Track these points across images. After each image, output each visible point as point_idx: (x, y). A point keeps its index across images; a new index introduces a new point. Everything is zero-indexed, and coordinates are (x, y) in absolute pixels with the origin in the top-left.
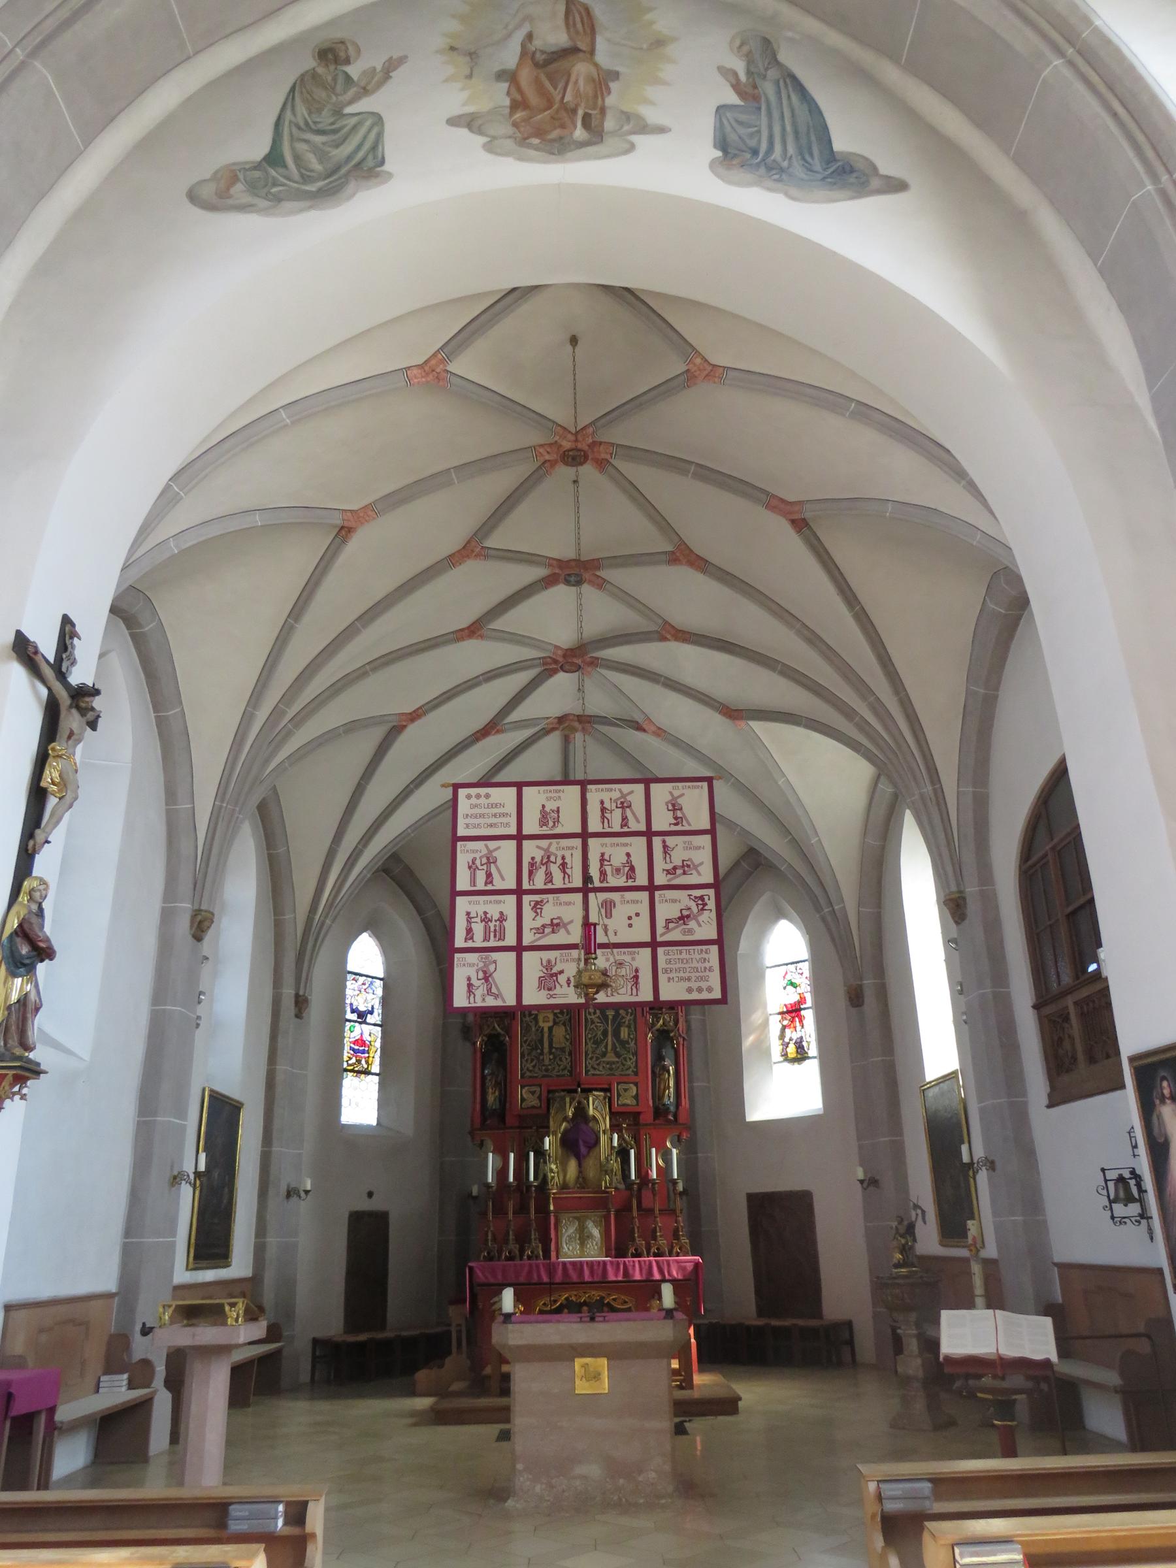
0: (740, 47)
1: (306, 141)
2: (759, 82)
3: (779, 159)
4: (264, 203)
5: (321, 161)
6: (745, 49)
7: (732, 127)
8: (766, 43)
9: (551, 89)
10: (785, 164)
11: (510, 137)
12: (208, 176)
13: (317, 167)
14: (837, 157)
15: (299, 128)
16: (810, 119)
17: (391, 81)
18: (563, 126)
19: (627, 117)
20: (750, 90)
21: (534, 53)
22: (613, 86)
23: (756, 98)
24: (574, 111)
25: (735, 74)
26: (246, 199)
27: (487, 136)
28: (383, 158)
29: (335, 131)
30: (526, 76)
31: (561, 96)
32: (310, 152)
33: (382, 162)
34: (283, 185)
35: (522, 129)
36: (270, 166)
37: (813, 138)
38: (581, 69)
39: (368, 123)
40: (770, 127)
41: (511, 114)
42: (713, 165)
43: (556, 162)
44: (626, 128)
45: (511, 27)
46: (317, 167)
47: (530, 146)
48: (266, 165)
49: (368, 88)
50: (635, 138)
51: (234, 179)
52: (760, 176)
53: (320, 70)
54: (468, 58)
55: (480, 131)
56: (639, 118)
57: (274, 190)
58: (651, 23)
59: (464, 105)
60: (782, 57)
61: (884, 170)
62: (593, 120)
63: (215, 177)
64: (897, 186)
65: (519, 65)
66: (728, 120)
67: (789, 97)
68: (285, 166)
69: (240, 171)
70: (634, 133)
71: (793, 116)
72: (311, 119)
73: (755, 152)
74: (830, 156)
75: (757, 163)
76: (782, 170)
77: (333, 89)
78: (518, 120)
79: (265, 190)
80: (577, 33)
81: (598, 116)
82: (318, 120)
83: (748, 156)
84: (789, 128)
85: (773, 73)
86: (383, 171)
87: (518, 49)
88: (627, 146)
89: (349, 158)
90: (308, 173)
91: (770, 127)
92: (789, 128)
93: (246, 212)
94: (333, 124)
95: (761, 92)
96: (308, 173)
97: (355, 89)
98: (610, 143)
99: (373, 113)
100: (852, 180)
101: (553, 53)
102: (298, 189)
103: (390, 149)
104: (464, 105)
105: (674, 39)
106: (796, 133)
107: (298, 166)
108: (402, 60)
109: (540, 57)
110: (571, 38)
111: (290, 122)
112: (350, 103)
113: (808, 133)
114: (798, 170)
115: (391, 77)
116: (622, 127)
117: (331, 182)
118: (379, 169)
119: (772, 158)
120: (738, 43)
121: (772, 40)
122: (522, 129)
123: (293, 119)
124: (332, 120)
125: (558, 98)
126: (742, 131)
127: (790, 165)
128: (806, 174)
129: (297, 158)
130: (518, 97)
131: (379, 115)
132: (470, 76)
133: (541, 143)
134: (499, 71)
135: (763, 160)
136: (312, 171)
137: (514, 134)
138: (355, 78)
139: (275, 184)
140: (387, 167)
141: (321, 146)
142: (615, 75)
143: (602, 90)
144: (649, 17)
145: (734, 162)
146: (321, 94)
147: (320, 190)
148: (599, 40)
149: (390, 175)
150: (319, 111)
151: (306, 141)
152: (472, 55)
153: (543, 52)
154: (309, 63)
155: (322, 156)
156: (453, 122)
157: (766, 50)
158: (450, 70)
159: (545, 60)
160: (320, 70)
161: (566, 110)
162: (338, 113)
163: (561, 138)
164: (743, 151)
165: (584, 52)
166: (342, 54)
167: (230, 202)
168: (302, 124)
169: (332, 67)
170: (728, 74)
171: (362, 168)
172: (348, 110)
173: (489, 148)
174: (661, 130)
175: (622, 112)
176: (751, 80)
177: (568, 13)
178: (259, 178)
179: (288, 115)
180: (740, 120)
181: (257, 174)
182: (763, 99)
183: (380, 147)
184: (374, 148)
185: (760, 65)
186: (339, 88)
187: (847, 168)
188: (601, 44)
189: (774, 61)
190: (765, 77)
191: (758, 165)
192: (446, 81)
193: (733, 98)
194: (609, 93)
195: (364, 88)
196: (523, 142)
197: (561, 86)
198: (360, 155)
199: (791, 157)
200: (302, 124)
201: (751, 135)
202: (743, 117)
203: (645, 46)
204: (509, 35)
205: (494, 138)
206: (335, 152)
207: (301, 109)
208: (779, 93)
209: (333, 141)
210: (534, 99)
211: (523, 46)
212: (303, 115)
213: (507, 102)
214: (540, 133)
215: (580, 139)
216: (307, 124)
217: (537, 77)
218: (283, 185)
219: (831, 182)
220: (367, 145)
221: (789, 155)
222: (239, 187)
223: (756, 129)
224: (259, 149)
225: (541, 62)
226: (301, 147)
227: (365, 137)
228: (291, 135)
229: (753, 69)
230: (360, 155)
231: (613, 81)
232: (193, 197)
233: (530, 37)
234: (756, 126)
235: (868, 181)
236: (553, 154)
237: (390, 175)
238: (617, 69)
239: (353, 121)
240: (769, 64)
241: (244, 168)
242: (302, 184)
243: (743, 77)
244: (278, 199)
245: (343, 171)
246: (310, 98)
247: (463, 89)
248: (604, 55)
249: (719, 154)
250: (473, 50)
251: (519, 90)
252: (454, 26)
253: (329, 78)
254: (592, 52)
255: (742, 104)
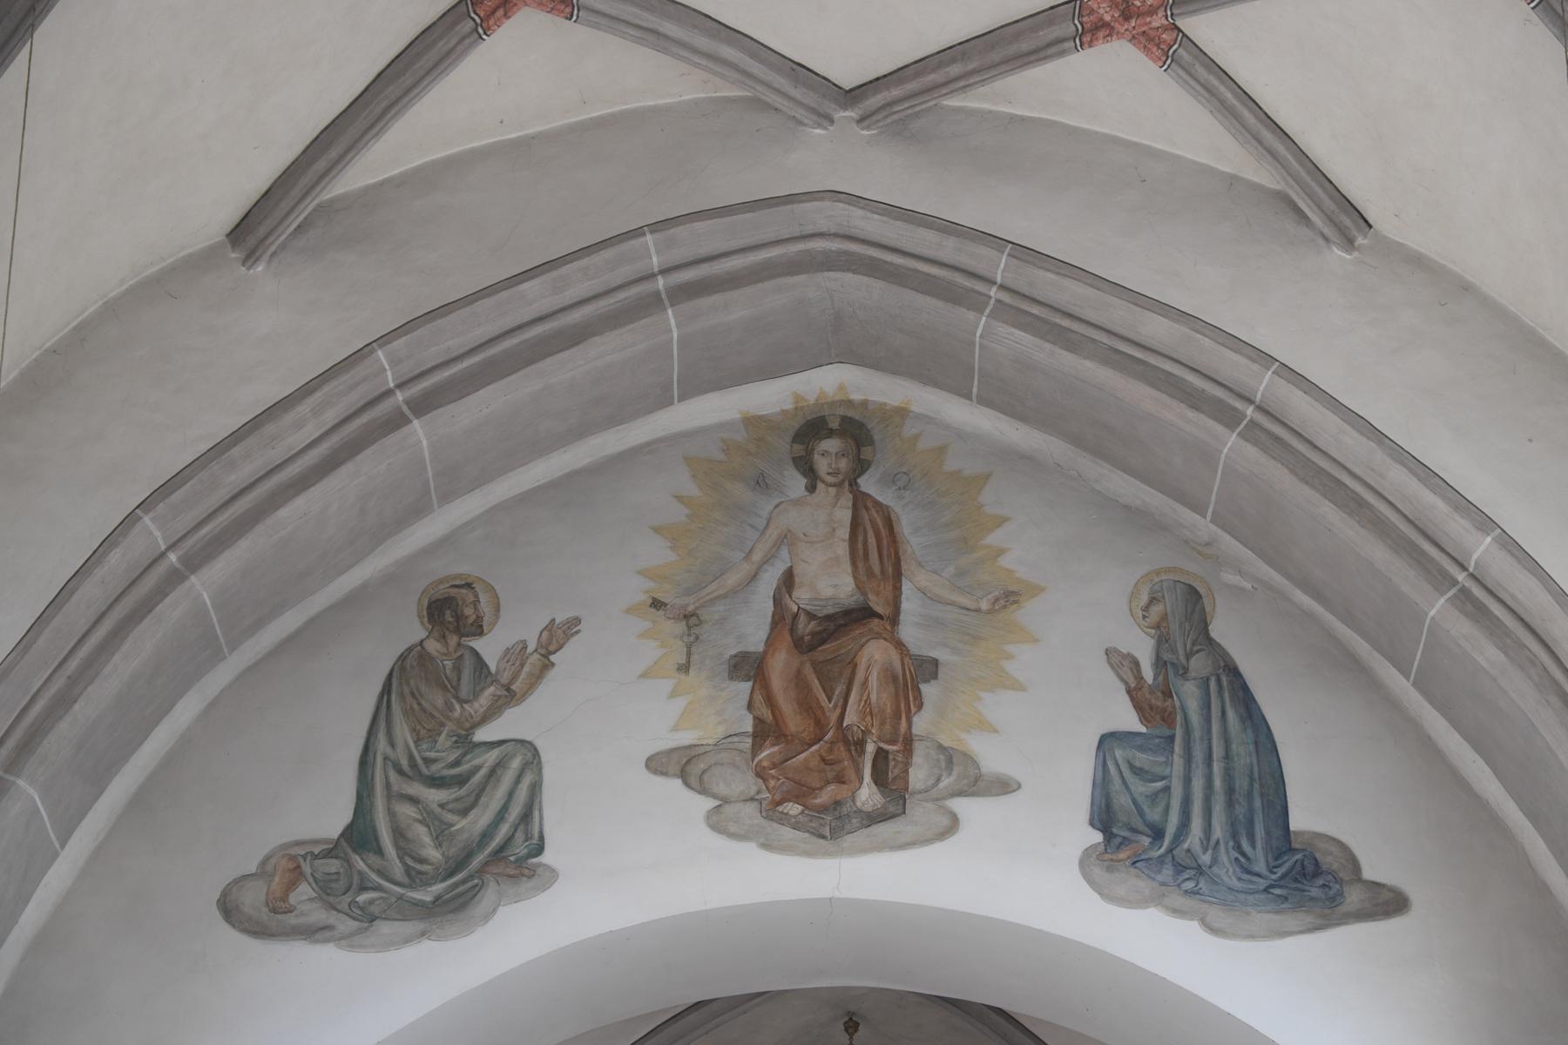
0: (1146, 608)
1: (413, 800)
2: (1176, 683)
3: (1197, 848)
4: (349, 925)
5: (438, 840)
6: (1157, 610)
7: (1124, 782)
8: (1193, 596)
9: (822, 697)
10: (1206, 859)
11: (752, 799)
12: (252, 868)
13: (433, 853)
14: (1295, 845)
15: (401, 772)
16: (1255, 762)
17: (552, 673)
18: (840, 780)
19: (949, 757)
20: (1158, 702)
21: (796, 616)
22: (929, 690)
23: (1167, 718)
24: (860, 745)
25: (1136, 664)
26: (318, 915)
27: (715, 796)
28: (542, 838)
29: (461, 781)
30: (780, 665)
31: (838, 711)
32: (420, 822)
33: (540, 849)
34: (378, 888)
35: (772, 783)
36: (354, 851)
37: (1258, 803)
38: (875, 655)
39: (516, 764)
40: (1187, 781)
41: (756, 749)
42: (1084, 864)
43: (827, 854)
44: (945, 783)
45: (757, 557)
46: (433, 853)
47: (784, 819)
48: (349, 850)
49: (513, 687)
50: (959, 805)
51: (296, 875)
52: (1163, 884)
53: (433, 646)
54: (681, 627)
55: (703, 791)
56: (969, 759)
57: (363, 898)
58: (1001, 552)
59: (676, 728)
60: (1215, 631)
61: (1368, 873)
62: (892, 764)
63: (263, 872)
64: (1389, 903)
65: (770, 642)
66: (1117, 765)
67: (1224, 713)
68: (380, 852)
69: (305, 860)
70: (961, 793)
71: (1227, 757)
72: (419, 752)
73: (1158, 834)
74: (1283, 840)
75: (1160, 857)
76: (1200, 870)
77: (456, 688)
78: (765, 764)
79: (347, 898)
80: (870, 574)
81: (900, 758)
82: (432, 755)
83: (1146, 841)
84: (1218, 783)
85: (1199, 664)
86: (540, 865)
87: (769, 607)
88: (945, 821)
89: (486, 835)
90: (418, 867)
91: (1187, 781)
92: (1218, 783)
93: (316, 941)
94: (457, 763)
95: (1177, 704)
96: (418, 867)
97: (492, 689)
98: (920, 813)
99: (522, 742)
100: (1315, 892)
101: (829, 618)
102: (401, 897)
103: (555, 822)
104: (676, 728)
105: (1036, 590)
106: (1230, 791)
107: (403, 852)
108: (571, 627)
109: (805, 627)
110: (859, 586)
111: (386, 758)
112: (485, 719)
113: (1250, 795)
114: (1227, 872)
115: (553, 664)
116: (938, 780)
117: (456, 885)
118: (535, 860)
119: (1186, 846)
120: (1145, 598)
121: (1202, 591)
122: (772, 783)
123: (389, 751)
124: (452, 757)
125: (833, 718)
126: (1140, 788)
127: (1215, 860)
128: (1240, 879)
129: (399, 834)
130: (767, 714)
131: (535, 749)
132: (684, 668)
133: (802, 812)
134: (736, 656)
135: (1170, 851)
136: (422, 861)
137: (758, 792)
138: (493, 669)
139: (363, 888)
140: (547, 858)
141: (438, 810)
142: (930, 668)
143: (907, 698)
144: (994, 538)
145: (1122, 856)
146: (437, 699)
147: (437, 898)
148: (907, 587)
149: (553, 874)
150: (433, 735)
151: (413, 800)
152: (690, 618)
153: (811, 616)
154: (414, 631)
155: (441, 835)
156: (657, 764)
157: (1193, 611)
158: (651, 652)
159: (813, 634)
160: (433, 646)
161: (846, 742)
162: (465, 742)
163: (837, 804)
164: (1141, 833)
165: (880, 617)
166: (469, 611)
167: (291, 920)
168: (404, 763)
169: (453, 640)
170: (1121, 662)
171: (506, 858)
172: (482, 735)
173: (716, 822)
174: (1004, 786)
175: (941, 748)
176: (1161, 678)
177: (855, 524)
178: (337, 873)
179: (382, 744)
180: (1137, 764)
181: (333, 865)
182: (1179, 718)
183: (536, 813)
184: (526, 817)
185: (1181, 652)
186: (464, 692)
187: (1310, 868)
188: (910, 604)
189: (1205, 640)
190: (1184, 673)
191: (1161, 860)
192: (644, 675)
193: (1129, 720)
194: (920, 706)
195: (508, 690)
196: (772, 811)
197: (839, 690)
198: (504, 830)
199: (1218, 842)
200: (404, 763)
201: (1154, 797)
202: (1142, 759)
203: (984, 605)
204: (754, 577)
205: (725, 801)
206: (461, 823)
207: (402, 731)
208: (1206, 706)
209: (456, 800)
210: (794, 722)
211: (777, 601)
212: (408, 747)
213: (748, 725)
214: (801, 792)
215: (868, 808)
216: (411, 758)
217: (799, 672)
218: (378, 888)
219: (1279, 896)
220: (515, 812)
221: (1213, 842)
222: (304, 891)
223: (1160, 784)
224: (333, 819)
225: (807, 638)
226: (407, 811)
227: (511, 795)
228: (388, 786)
229: (1166, 656)
230: (504, 830)
231: (927, 681)
232: (228, 909)
233: (788, 581)
234: (1163, 778)
235: (1341, 894)
236: (823, 837)
237: (553, 874)
238: (934, 654)
239: (492, 757)
240: (1194, 644)
241: (312, 853)
242: (410, 887)
243: (1148, 674)
244: (369, 918)
245: (477, 862)
246: (416, 706)
247: (673, 695)
248: (910, 631)
249: (1098, 837)
250: (691, 608)
251: (770, 700)
252: (657, 553)
253: (449, 664)
254: (894, 619)
255: (1143, 729)
